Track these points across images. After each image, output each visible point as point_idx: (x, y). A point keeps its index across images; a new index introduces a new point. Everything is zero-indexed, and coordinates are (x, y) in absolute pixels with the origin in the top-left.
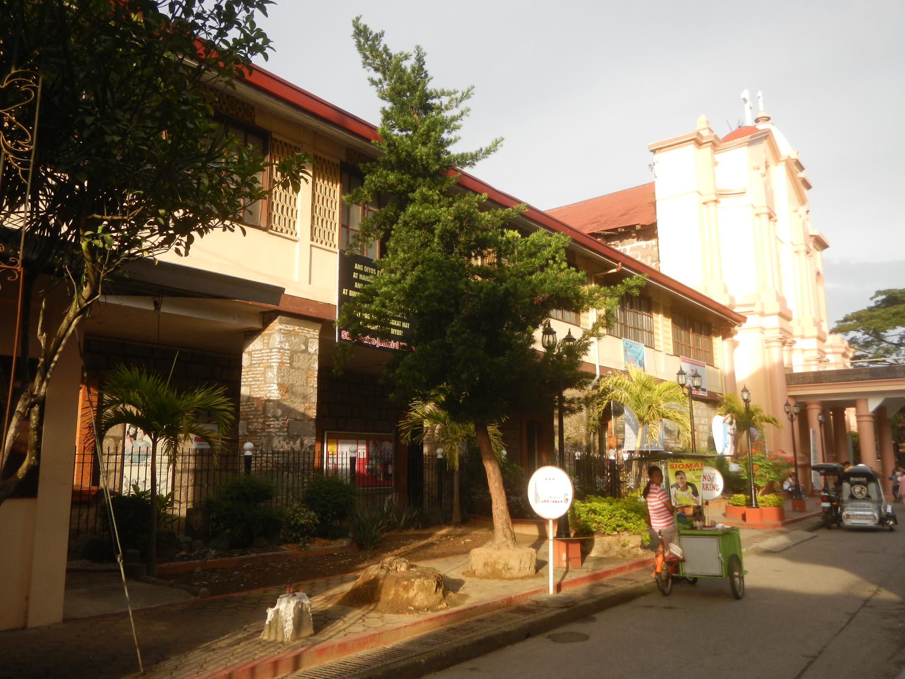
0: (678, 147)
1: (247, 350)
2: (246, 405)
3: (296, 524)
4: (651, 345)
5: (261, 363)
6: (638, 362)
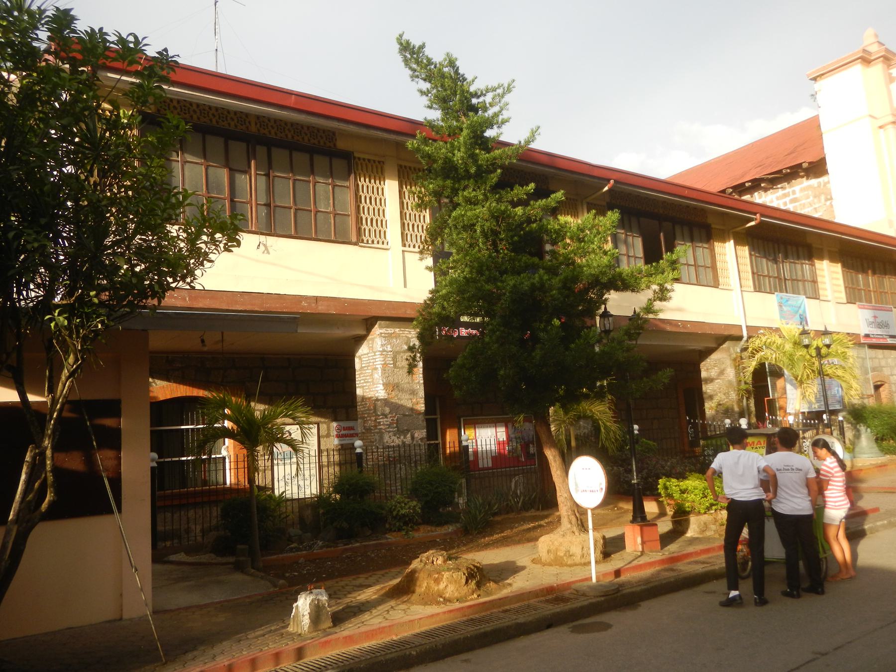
0: (843, 70)
1: (357, 355)
2: (361, 405)
3: (397, 514)
4: (815, 296)
5: (369, 366)
6: (798, 316)
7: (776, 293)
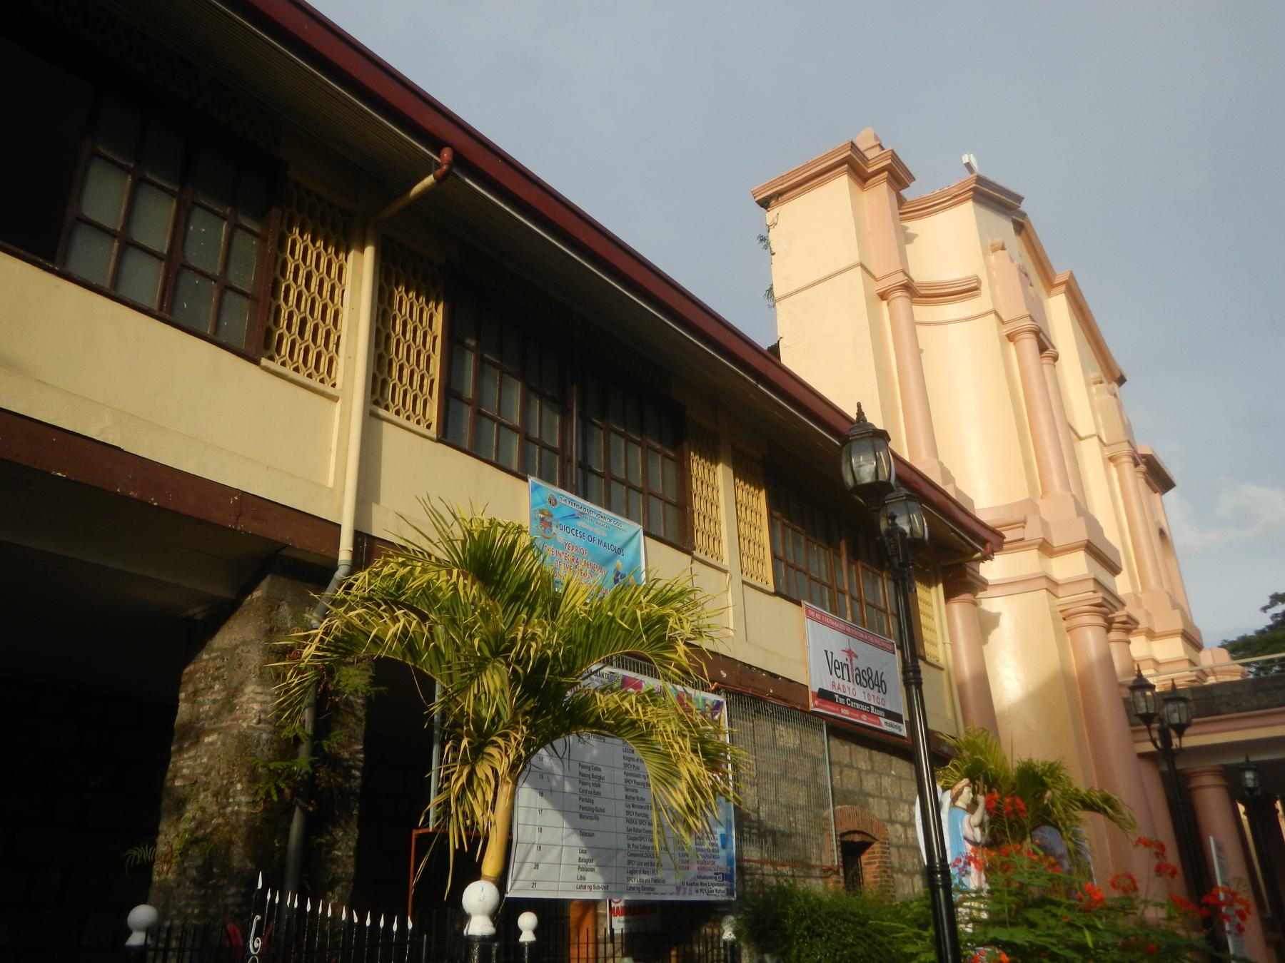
7: (531, 479)
